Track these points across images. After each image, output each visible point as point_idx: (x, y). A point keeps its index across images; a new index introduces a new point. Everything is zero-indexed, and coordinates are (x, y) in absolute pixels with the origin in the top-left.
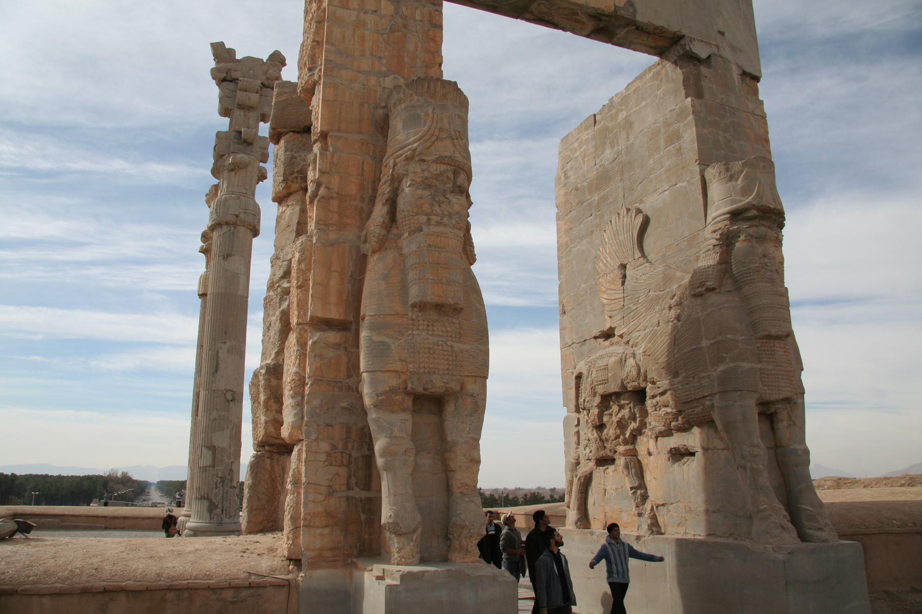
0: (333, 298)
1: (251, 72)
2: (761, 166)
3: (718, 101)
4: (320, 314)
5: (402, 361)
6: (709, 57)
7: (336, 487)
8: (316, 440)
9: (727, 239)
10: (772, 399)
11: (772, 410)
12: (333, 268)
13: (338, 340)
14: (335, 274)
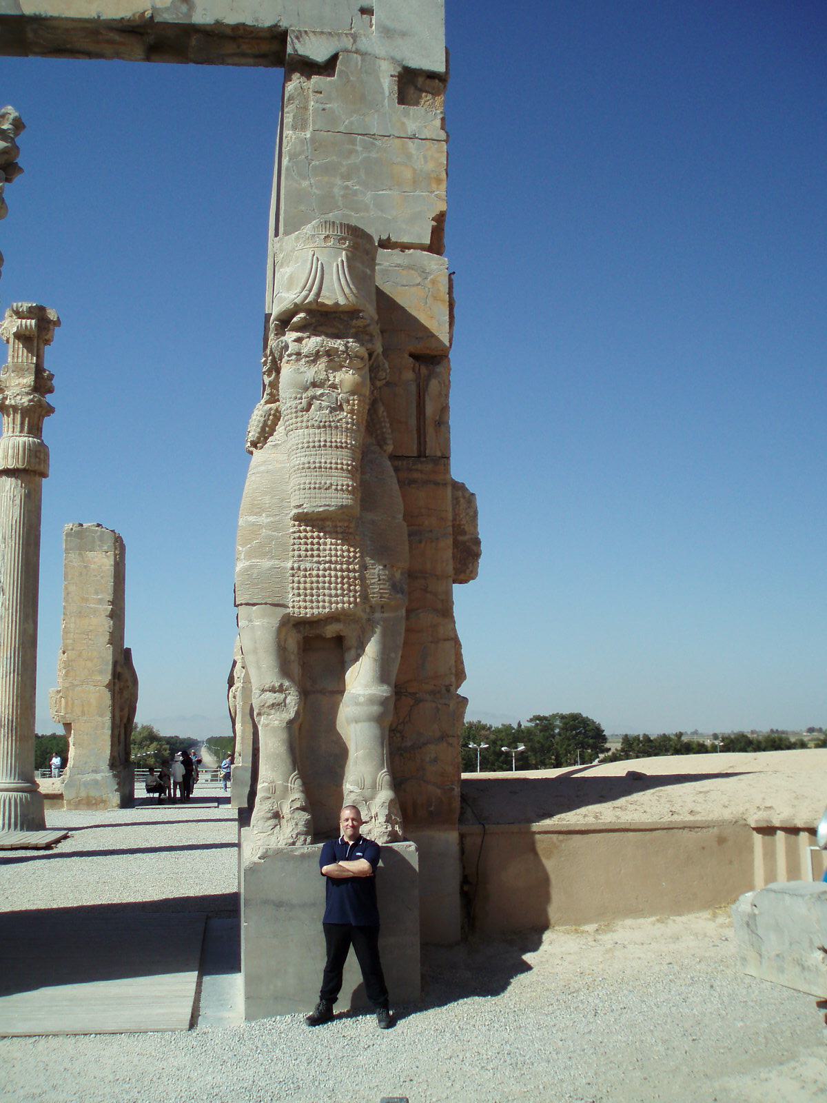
2: (323, 236)
3: (342, 129)
9: (274, 361)
10: (308, 616)
11: (330, 630)
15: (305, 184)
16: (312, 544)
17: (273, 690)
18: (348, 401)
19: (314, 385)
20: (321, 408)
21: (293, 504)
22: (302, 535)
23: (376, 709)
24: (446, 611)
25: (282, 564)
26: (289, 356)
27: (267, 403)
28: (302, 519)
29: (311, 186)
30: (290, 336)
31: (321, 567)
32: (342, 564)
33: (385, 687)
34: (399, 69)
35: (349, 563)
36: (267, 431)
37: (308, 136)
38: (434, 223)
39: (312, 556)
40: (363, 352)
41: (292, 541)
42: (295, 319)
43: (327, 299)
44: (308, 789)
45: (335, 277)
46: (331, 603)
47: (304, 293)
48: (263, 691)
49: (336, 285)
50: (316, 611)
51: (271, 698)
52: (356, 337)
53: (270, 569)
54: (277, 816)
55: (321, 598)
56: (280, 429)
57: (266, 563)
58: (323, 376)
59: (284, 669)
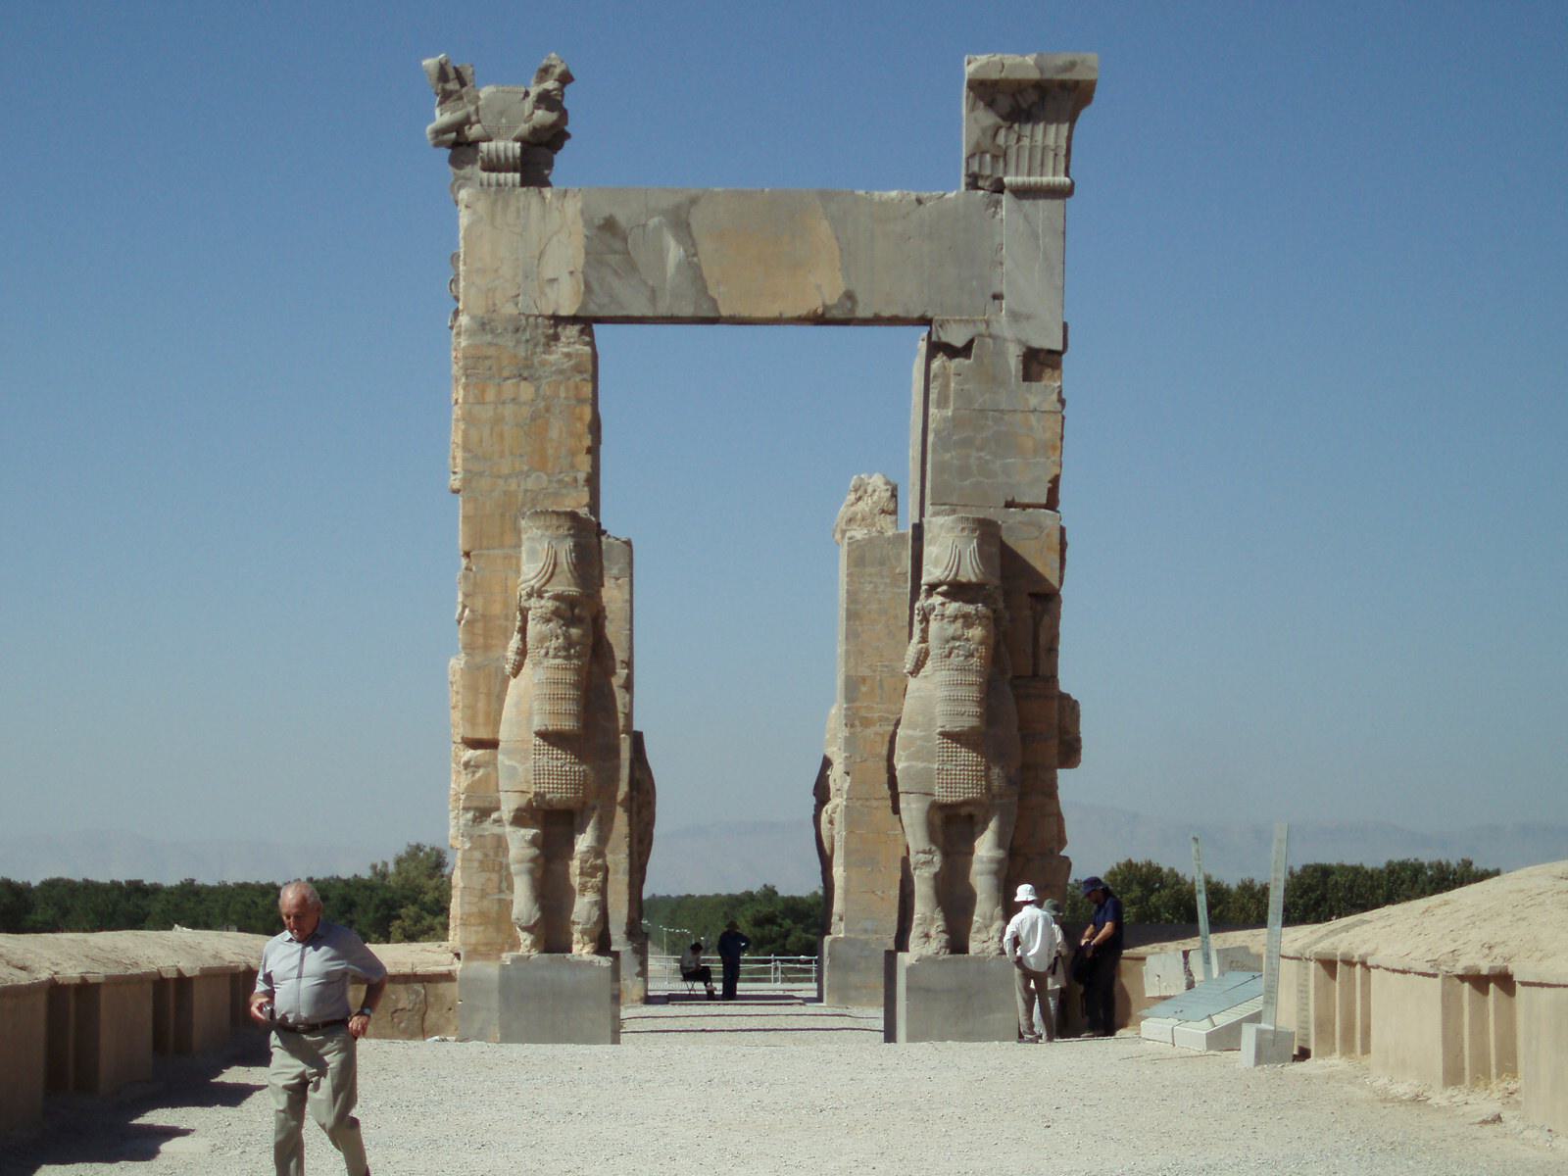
0: (481, 719)
1: (504, 121)
2: (960, 528)
4: (470, 735)
5: (526, 782)
6: (971, 342)
7: (488, 890)
8: (470, 849)
11: (964, 811)
12: (481, 690)
13: (487, 758)
14: (482, 697)
15: (947, 456)
16: (952, 752)
17: (924, 852)
18: (977, 650)
19: (954, 638)
20: (958, 656)
21: (939, 724)
22: (945, 745)
23: (994, 866)
24: (1051, 791)
25: (931, 766)
26: (936, 616)
27: (920, 642)
28: (945, 735)
29: (952, 457)
30: (937, 600)
31: (958, 768)
32: (972, 766)
33: (1001, 851)
34: (1024, 350)
35: (977, 765)
36: (919, 665)
37: (950, 414)
38: (1050, 485)
39: (952, 761)
40: (989, 613)
41: (937, 750)
42: (940, 590)
43: (963, 578)
44: (947, 919)
45: (968, 560)
46: (964, 793)
47: (947, 573)
48: (918, 853)
49: (969, 567)
50: (954, 799)
51: (922, 857)
52: (985, 604)
53: (922, 769)
54: (927, 936)
55: (958, 790)
56: (929, 663)
57: (920, 765)
58: (959, 632)
59: (932, 837)
